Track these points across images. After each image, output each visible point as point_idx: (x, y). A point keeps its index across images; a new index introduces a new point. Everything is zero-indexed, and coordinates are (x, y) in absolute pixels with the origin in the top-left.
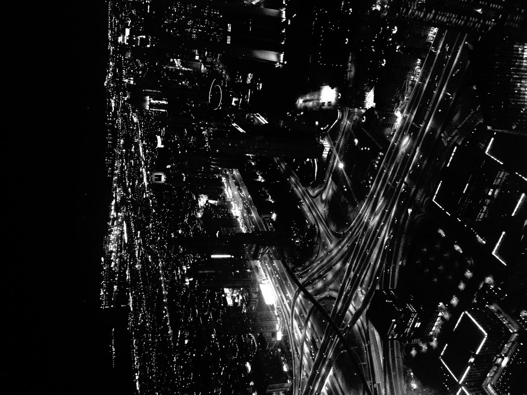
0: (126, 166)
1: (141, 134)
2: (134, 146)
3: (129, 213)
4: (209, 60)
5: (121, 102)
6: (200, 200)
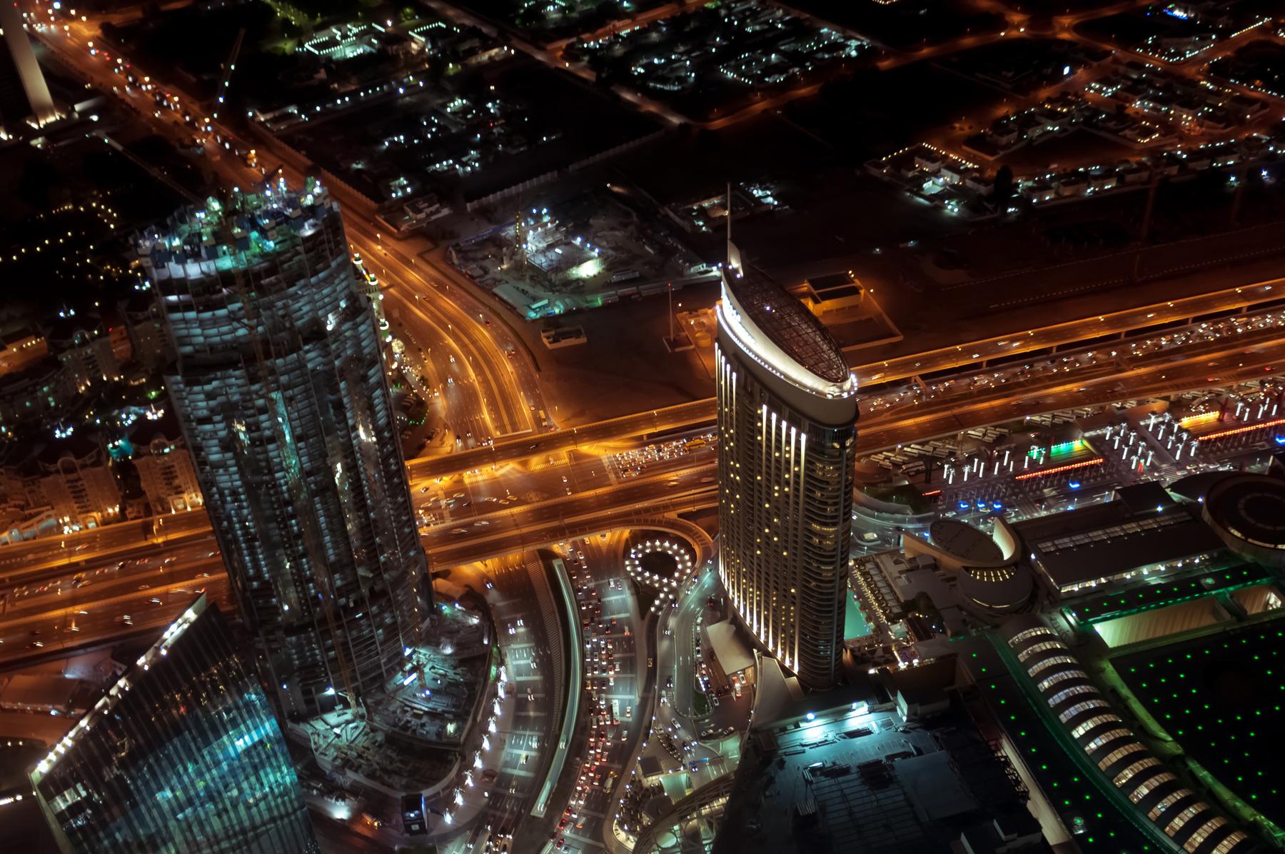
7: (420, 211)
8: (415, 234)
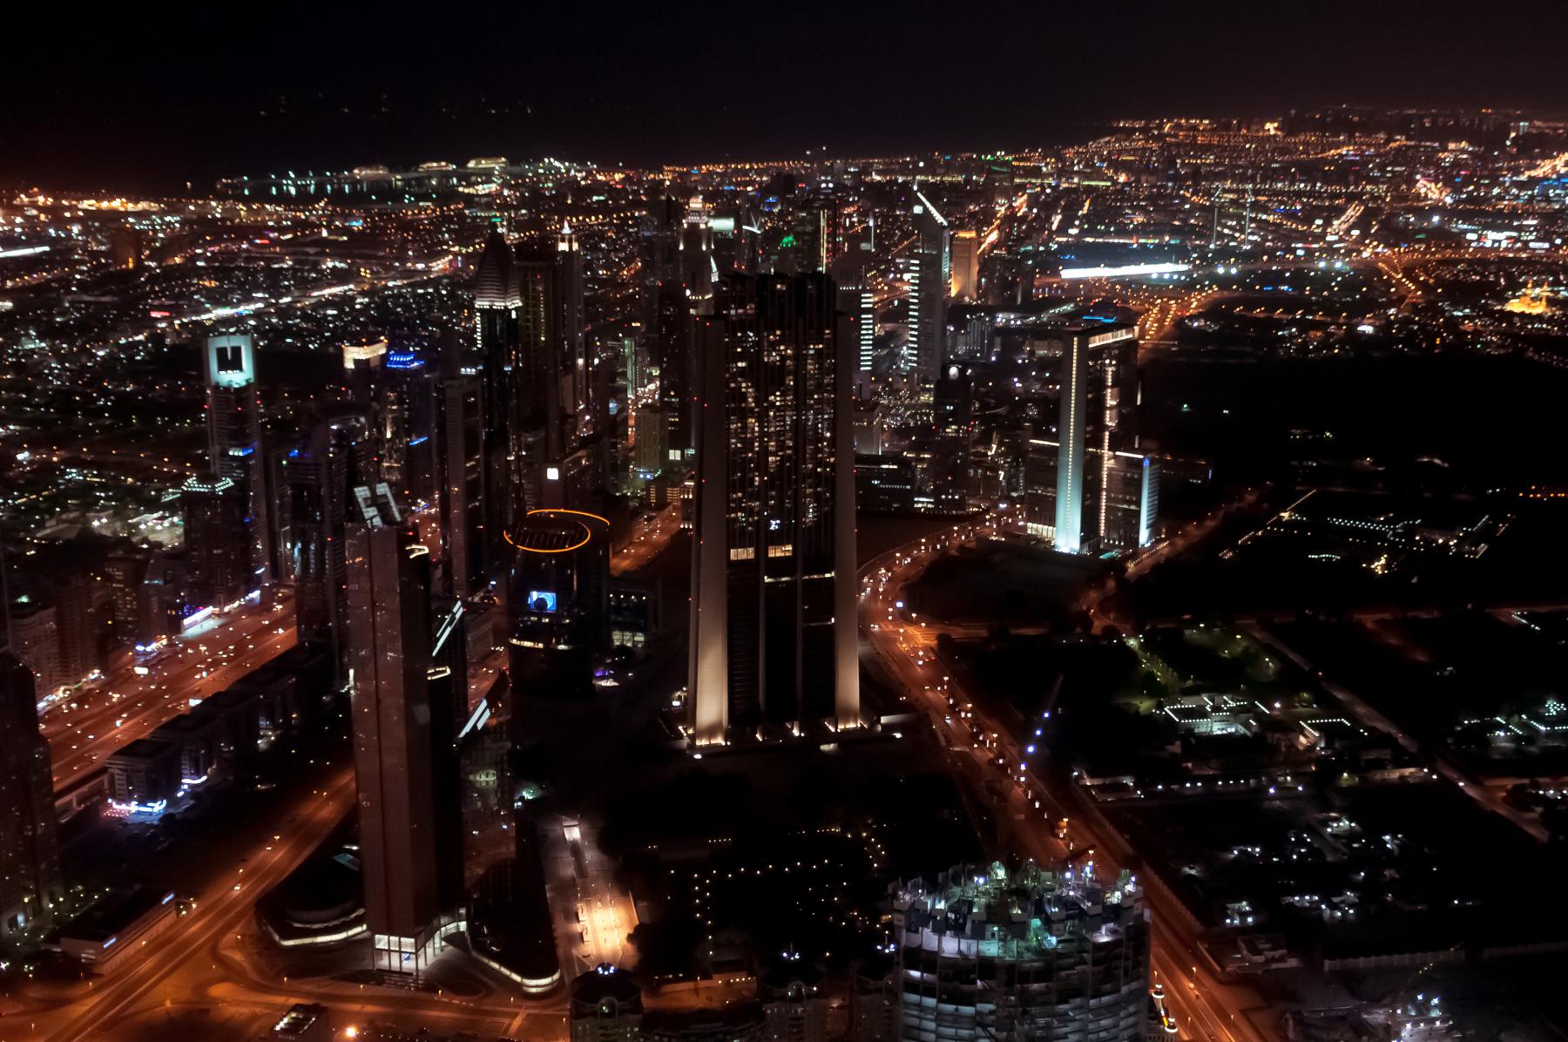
0: (267, 242)
1: (391, 289)
2: (343, 265)
3: (83, 262)
4: (673, 494)
5: (495, 217)
6: (162, 518)
7: (1259, 953)
8: (1243, 981)
